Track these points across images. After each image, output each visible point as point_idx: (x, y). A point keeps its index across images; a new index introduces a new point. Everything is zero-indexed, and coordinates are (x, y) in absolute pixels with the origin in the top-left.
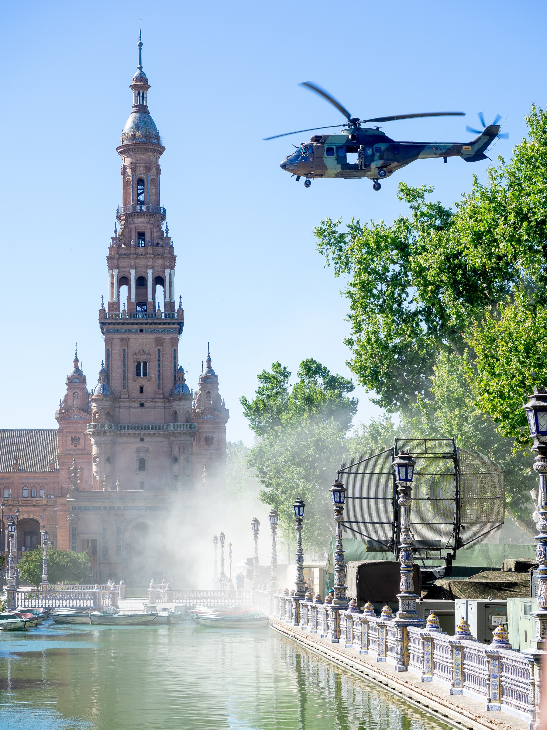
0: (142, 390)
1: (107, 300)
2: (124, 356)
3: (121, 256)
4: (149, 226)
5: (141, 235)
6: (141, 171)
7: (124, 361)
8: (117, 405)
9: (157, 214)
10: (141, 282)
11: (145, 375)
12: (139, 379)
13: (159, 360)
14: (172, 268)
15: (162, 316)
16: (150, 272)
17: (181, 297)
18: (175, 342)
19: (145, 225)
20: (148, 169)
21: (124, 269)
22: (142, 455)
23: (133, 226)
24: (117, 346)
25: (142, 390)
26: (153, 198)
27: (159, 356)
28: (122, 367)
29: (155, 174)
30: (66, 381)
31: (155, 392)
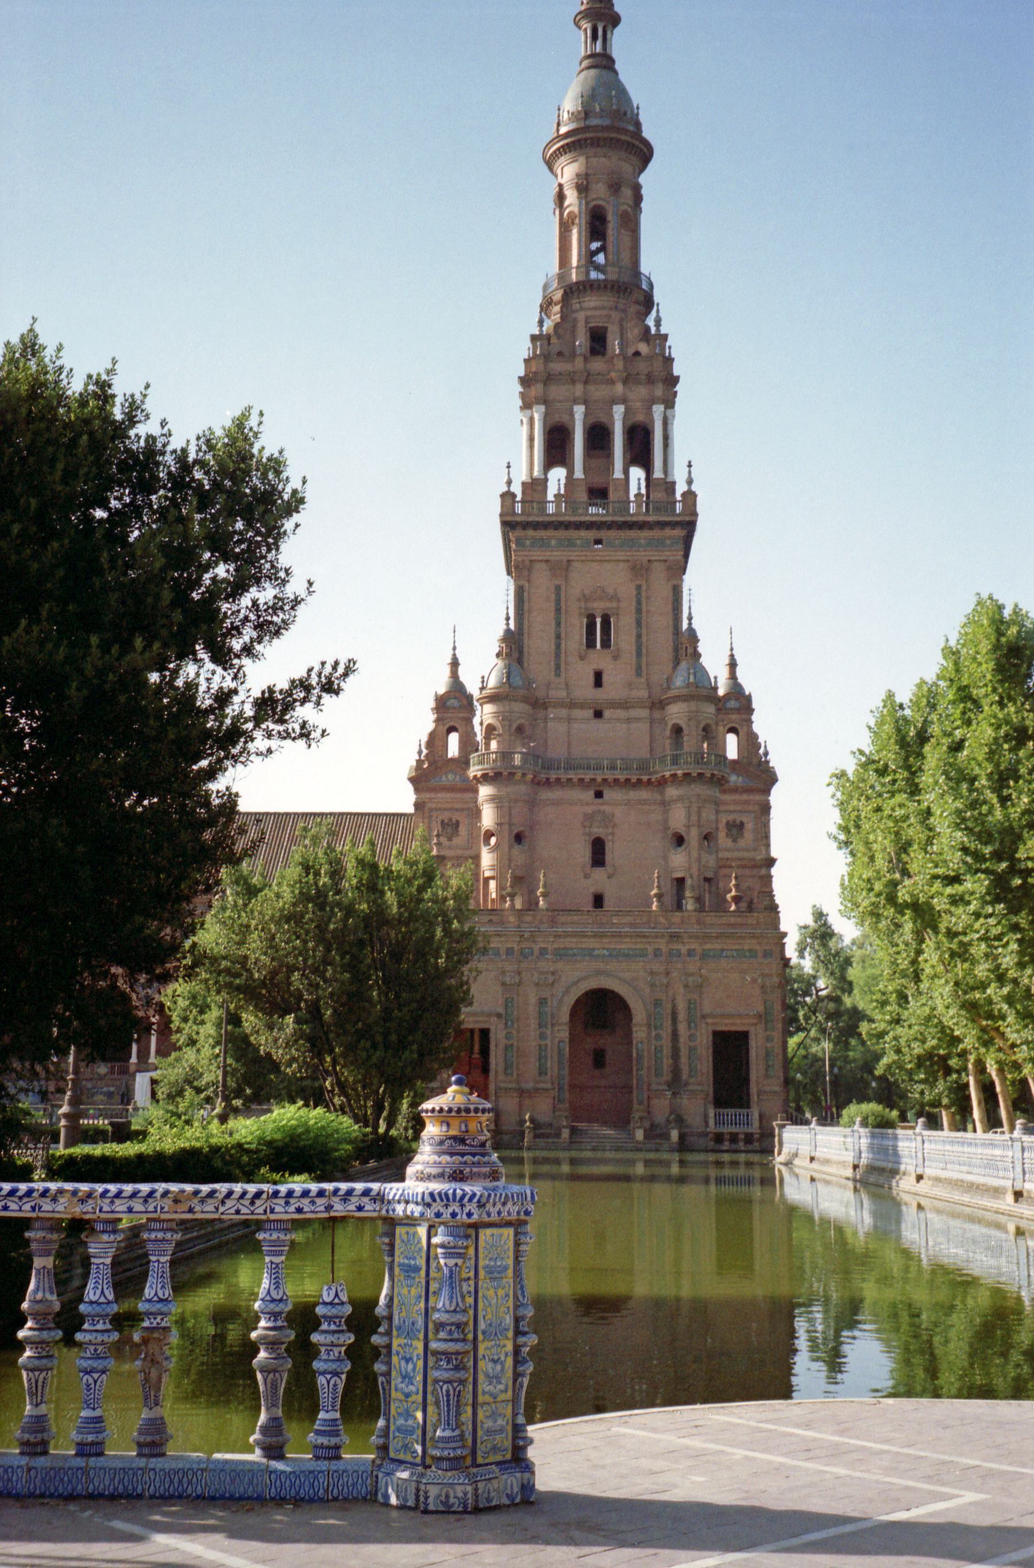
0: (598, 680)
1: (521, 475)
2: (558, 601)
4: (615, 315)
5: (598, 340)
7: (558, 610)
8: (541, 714)
9: (635, 294)
10: (598, 437)
11: (606, 644)
12: (592, 654)
13: (639, 611)
14: (669, 403)
16: (619, 411)
17: (690, 466)
19: (605, 312)
20: (615, 188)
22: (598, 831)
23: (581, 316)
24: (543, 581)
25: (598, 680)
26: (626, 256)
27: (639, 603)
30: (432, 704)
31: (630, 685)
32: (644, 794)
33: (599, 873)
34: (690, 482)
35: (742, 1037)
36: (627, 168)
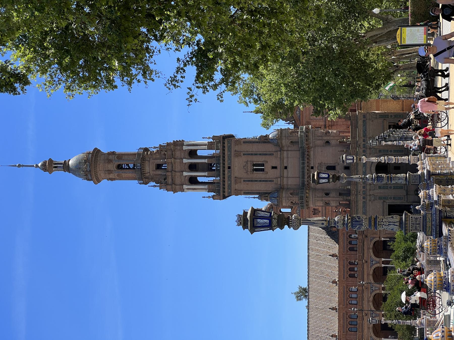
0: (274, 168)
2: (249, 181)
3: (173, 183)
4: (152, 161)
5: (159, 167)
6: (112, 167)
7: (252, 181)
10: (193, 167)
11: (263, 165)
13: (252, 154)
15: (218, 151)
16: (185, 161)
18: (239, 142)
19: (150, 164)
20: (110, 161)
21: (183, 180)
23: (152, 173)
25: (274, 168)
26: (131, 157)
27: (249, 154)
28: (257, 182)
29: (114, 156)
32: (312, 153)
33: (338, 168)
34: (209, 138)
35: (390, 206)
36: (102, 157)
